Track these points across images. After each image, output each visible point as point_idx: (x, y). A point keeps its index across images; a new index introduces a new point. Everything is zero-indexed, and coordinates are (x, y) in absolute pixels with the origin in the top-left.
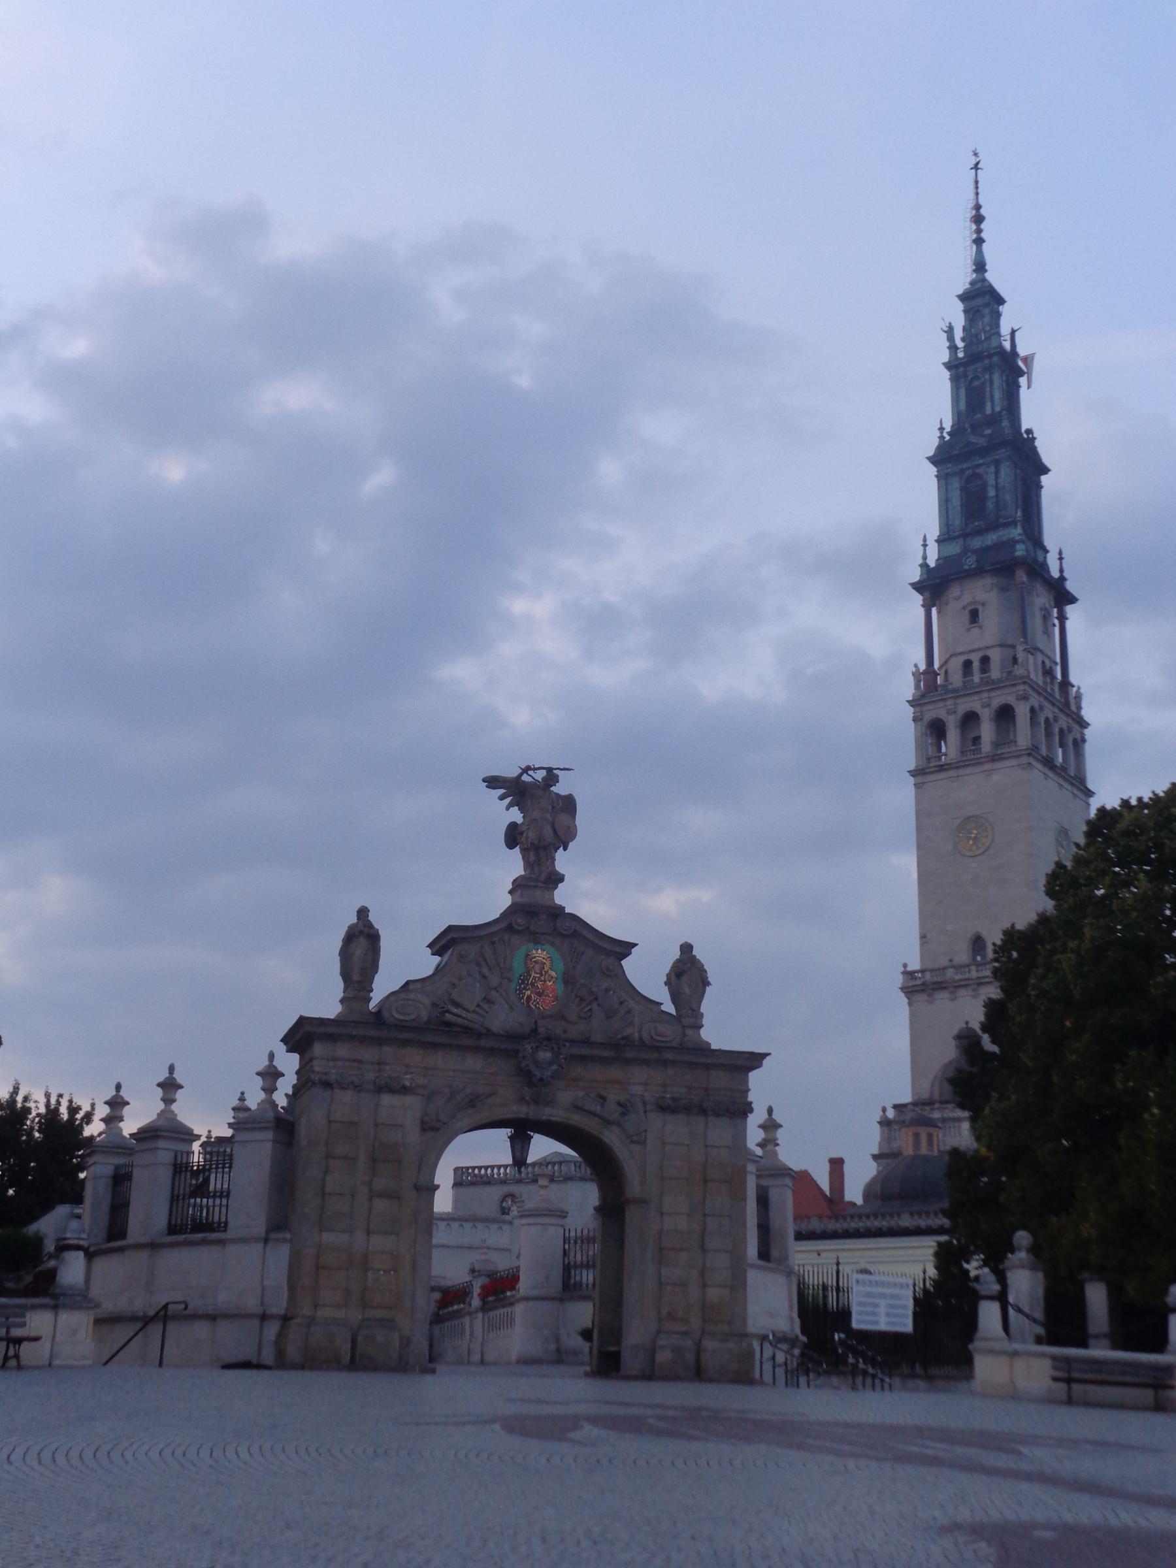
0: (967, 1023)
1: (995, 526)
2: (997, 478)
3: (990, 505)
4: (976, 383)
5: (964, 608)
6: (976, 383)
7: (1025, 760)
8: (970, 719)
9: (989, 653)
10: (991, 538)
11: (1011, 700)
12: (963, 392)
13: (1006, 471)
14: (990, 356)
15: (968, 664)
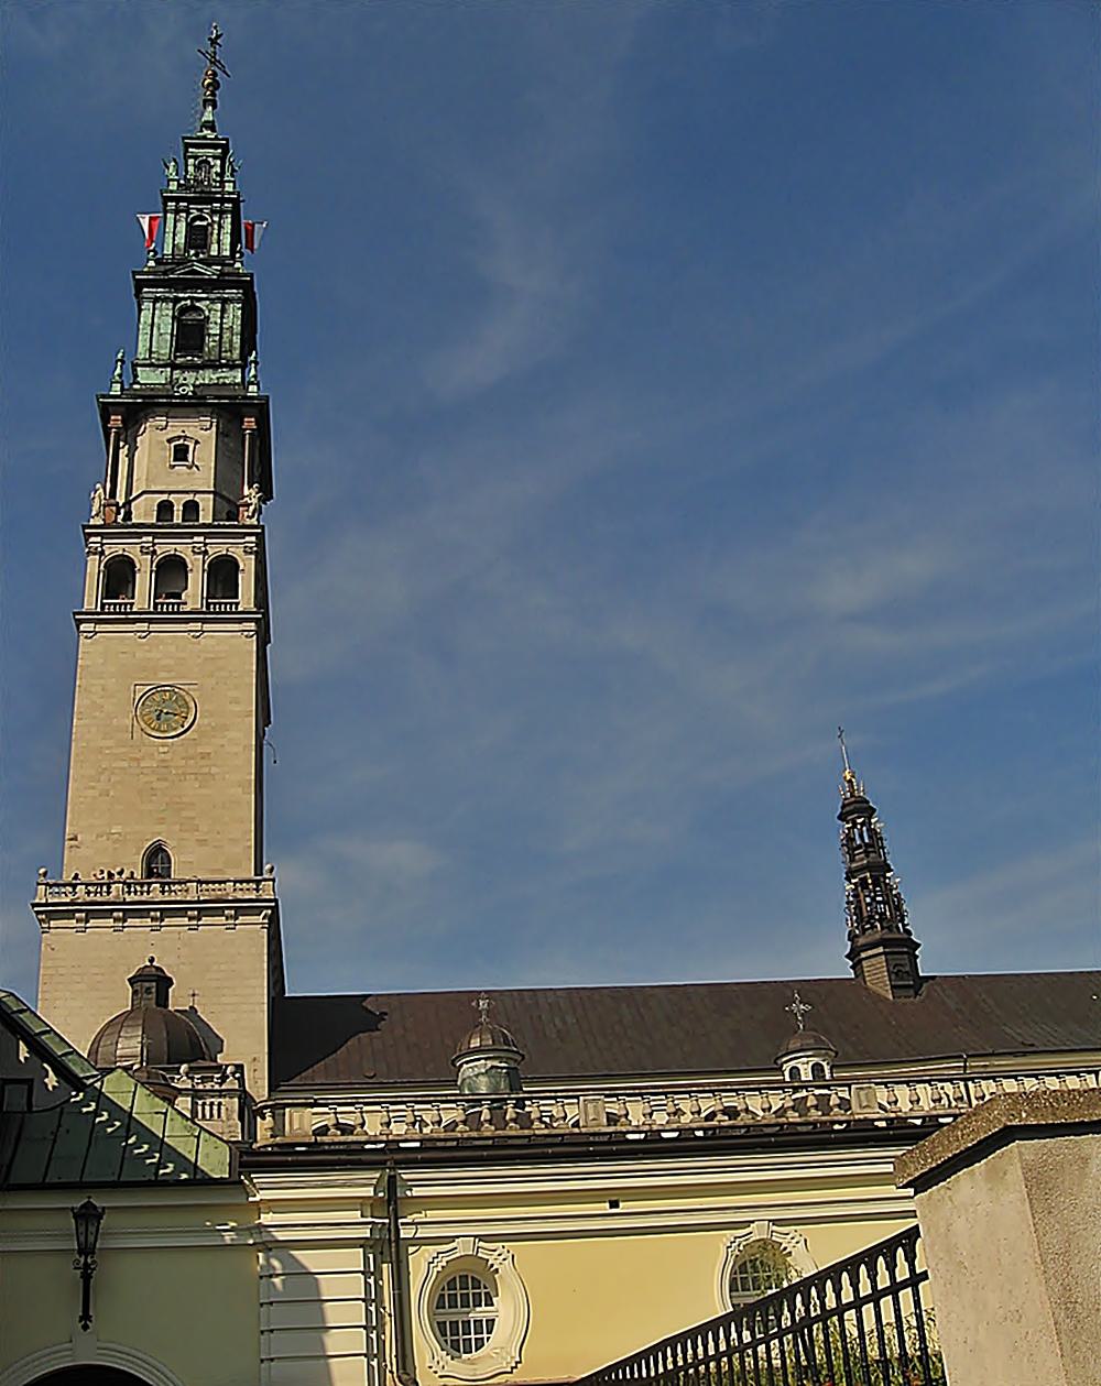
0: (152, 960)
1: (214, 366)
2: (222, 318)
3: (210, 343)
4: (198, 223)
5: (169, 441)
6: (198, 223)
7: (252, 626)
8: (171, 570)
9: (198, 498)
10: (209, 376)
11: (237, 552)
12: (182, 226)
13: (235, 313)
14: (222, 201)
15: (165, 509)
